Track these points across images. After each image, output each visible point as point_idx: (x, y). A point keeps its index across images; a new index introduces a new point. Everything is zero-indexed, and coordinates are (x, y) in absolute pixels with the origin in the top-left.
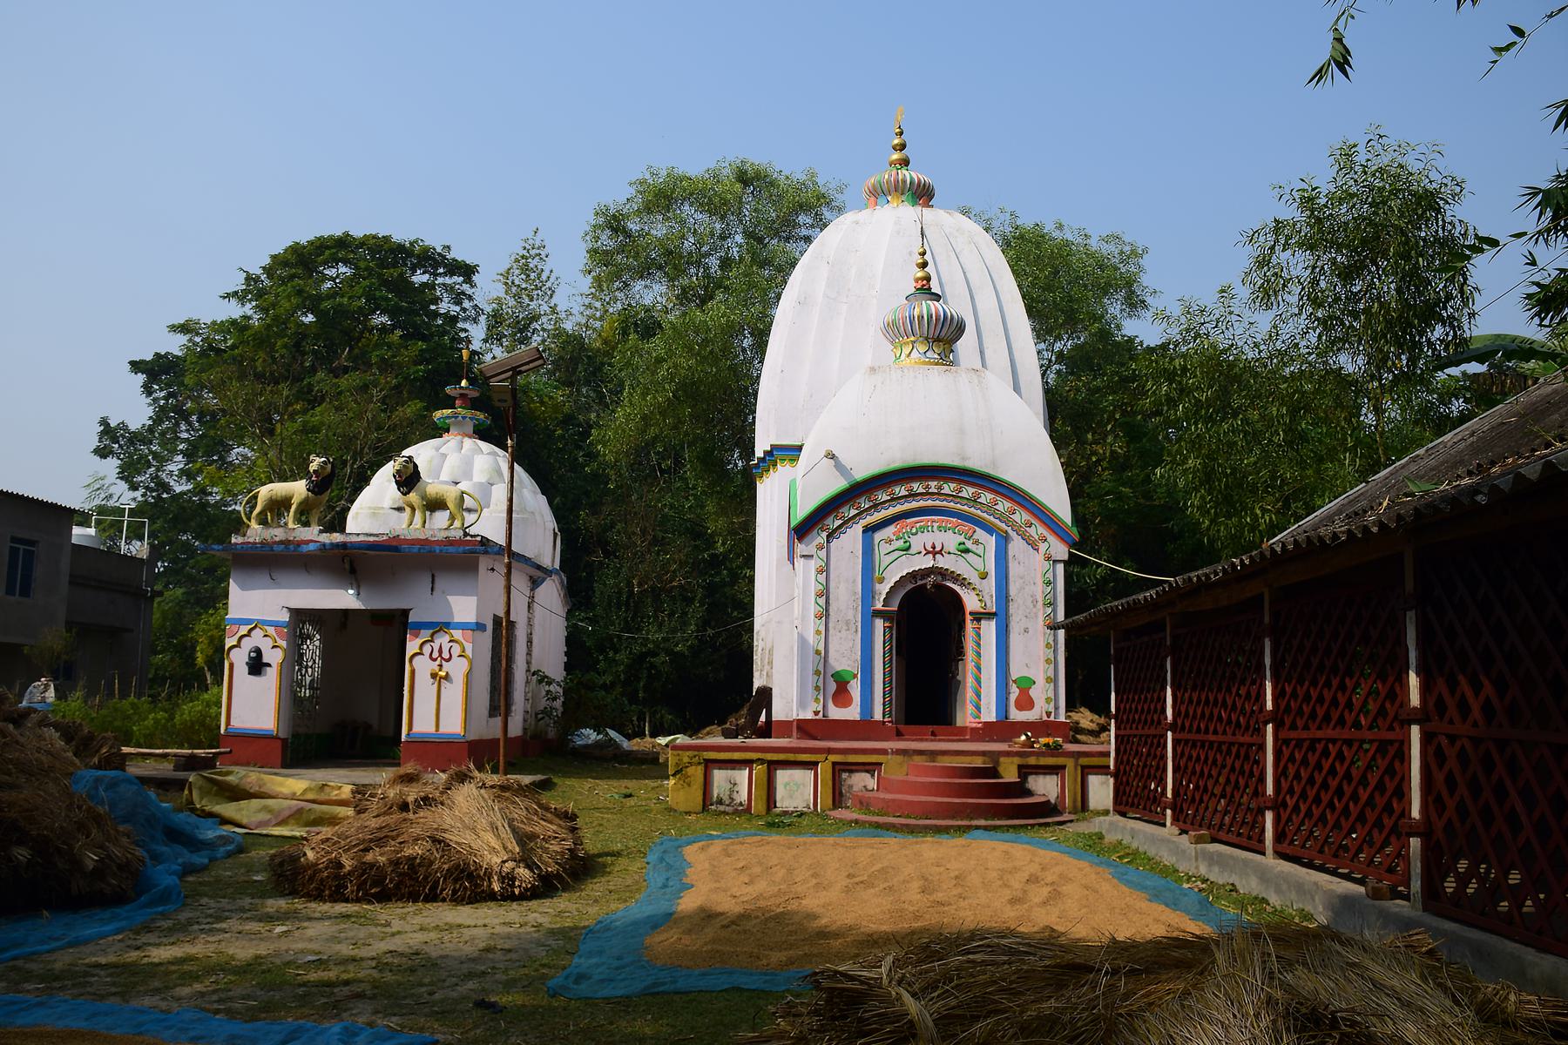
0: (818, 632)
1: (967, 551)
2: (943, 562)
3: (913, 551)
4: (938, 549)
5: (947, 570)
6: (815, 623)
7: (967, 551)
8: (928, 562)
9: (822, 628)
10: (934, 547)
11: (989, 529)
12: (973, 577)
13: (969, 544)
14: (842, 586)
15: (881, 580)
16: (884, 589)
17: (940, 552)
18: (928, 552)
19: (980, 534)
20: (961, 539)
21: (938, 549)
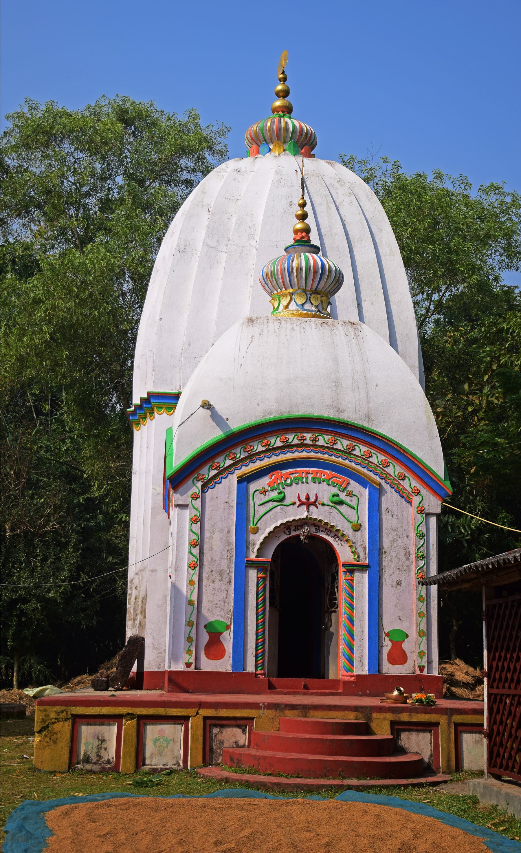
0: (191, 583)
1: (341, 503)
2: (316, 514)
3: (287, 501)
4: (312, 500)
5: (320, 521)
6: (188, 573)
7: (341, 503)
8: (302, 513)
9: (196, 579)
10: (308, 498)
11: (363, 482)
12: (347, 529)
13: (343, 496)
14: (217, 536)
15: (256, 531)
16: (258, 539)
17: (314, 504)
18: (302, 504)
19: (354, 486)
20: (335, 490)
21: (312, 500)
